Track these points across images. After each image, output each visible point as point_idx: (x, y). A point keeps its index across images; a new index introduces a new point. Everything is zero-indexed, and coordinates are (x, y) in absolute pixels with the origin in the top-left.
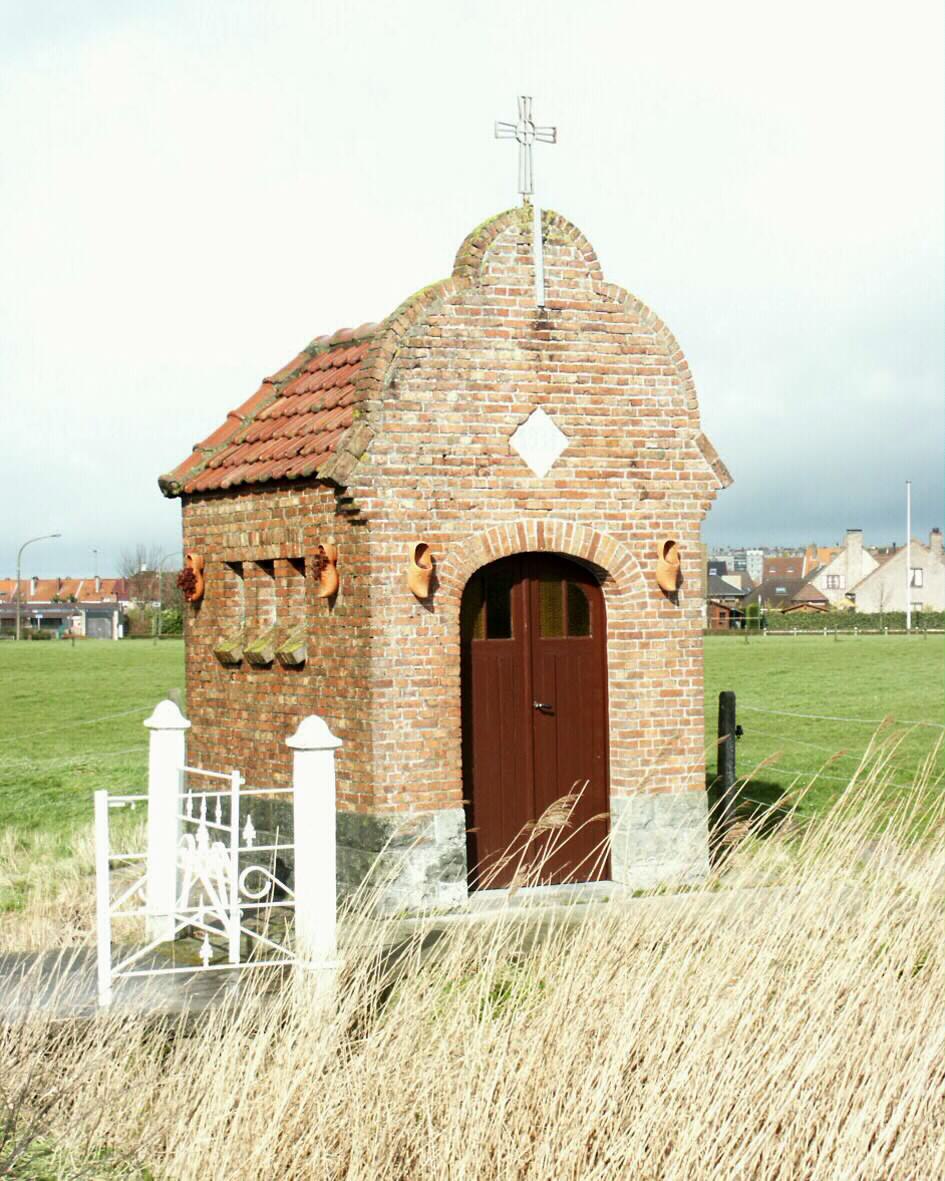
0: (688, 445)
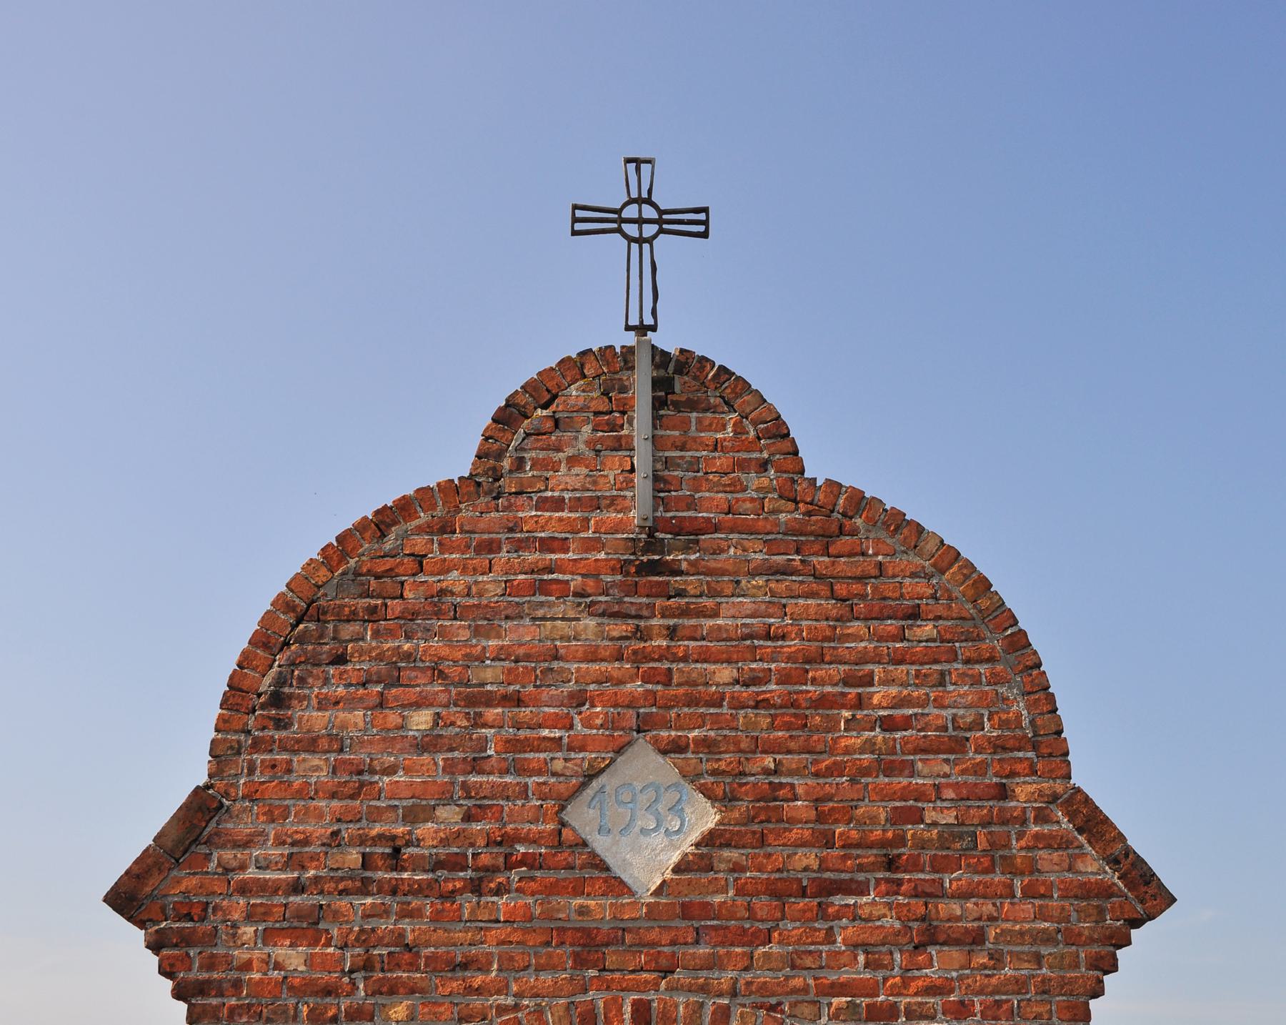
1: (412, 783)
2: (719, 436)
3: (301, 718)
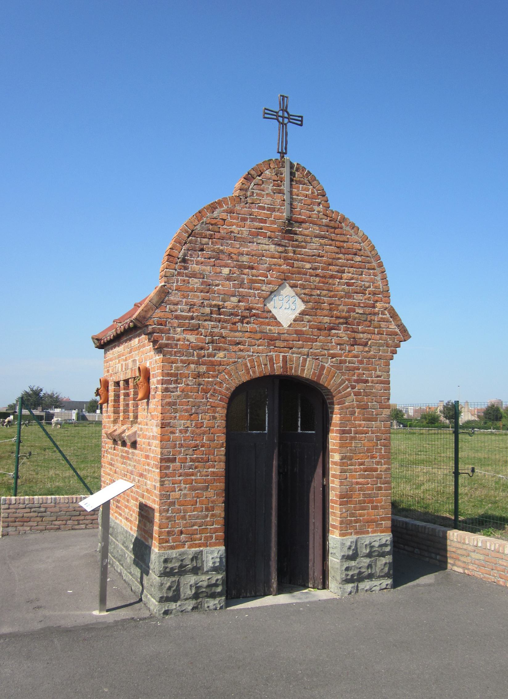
0: (383, 314)
1: (224, 290)
2: (307, 193)
3: (191, 267)
